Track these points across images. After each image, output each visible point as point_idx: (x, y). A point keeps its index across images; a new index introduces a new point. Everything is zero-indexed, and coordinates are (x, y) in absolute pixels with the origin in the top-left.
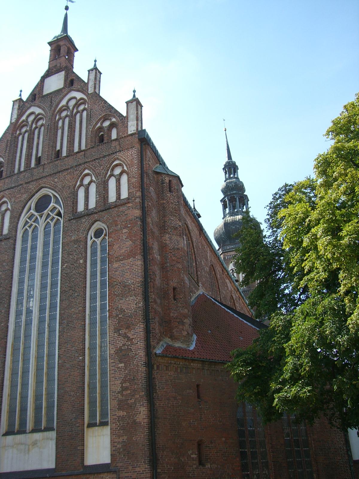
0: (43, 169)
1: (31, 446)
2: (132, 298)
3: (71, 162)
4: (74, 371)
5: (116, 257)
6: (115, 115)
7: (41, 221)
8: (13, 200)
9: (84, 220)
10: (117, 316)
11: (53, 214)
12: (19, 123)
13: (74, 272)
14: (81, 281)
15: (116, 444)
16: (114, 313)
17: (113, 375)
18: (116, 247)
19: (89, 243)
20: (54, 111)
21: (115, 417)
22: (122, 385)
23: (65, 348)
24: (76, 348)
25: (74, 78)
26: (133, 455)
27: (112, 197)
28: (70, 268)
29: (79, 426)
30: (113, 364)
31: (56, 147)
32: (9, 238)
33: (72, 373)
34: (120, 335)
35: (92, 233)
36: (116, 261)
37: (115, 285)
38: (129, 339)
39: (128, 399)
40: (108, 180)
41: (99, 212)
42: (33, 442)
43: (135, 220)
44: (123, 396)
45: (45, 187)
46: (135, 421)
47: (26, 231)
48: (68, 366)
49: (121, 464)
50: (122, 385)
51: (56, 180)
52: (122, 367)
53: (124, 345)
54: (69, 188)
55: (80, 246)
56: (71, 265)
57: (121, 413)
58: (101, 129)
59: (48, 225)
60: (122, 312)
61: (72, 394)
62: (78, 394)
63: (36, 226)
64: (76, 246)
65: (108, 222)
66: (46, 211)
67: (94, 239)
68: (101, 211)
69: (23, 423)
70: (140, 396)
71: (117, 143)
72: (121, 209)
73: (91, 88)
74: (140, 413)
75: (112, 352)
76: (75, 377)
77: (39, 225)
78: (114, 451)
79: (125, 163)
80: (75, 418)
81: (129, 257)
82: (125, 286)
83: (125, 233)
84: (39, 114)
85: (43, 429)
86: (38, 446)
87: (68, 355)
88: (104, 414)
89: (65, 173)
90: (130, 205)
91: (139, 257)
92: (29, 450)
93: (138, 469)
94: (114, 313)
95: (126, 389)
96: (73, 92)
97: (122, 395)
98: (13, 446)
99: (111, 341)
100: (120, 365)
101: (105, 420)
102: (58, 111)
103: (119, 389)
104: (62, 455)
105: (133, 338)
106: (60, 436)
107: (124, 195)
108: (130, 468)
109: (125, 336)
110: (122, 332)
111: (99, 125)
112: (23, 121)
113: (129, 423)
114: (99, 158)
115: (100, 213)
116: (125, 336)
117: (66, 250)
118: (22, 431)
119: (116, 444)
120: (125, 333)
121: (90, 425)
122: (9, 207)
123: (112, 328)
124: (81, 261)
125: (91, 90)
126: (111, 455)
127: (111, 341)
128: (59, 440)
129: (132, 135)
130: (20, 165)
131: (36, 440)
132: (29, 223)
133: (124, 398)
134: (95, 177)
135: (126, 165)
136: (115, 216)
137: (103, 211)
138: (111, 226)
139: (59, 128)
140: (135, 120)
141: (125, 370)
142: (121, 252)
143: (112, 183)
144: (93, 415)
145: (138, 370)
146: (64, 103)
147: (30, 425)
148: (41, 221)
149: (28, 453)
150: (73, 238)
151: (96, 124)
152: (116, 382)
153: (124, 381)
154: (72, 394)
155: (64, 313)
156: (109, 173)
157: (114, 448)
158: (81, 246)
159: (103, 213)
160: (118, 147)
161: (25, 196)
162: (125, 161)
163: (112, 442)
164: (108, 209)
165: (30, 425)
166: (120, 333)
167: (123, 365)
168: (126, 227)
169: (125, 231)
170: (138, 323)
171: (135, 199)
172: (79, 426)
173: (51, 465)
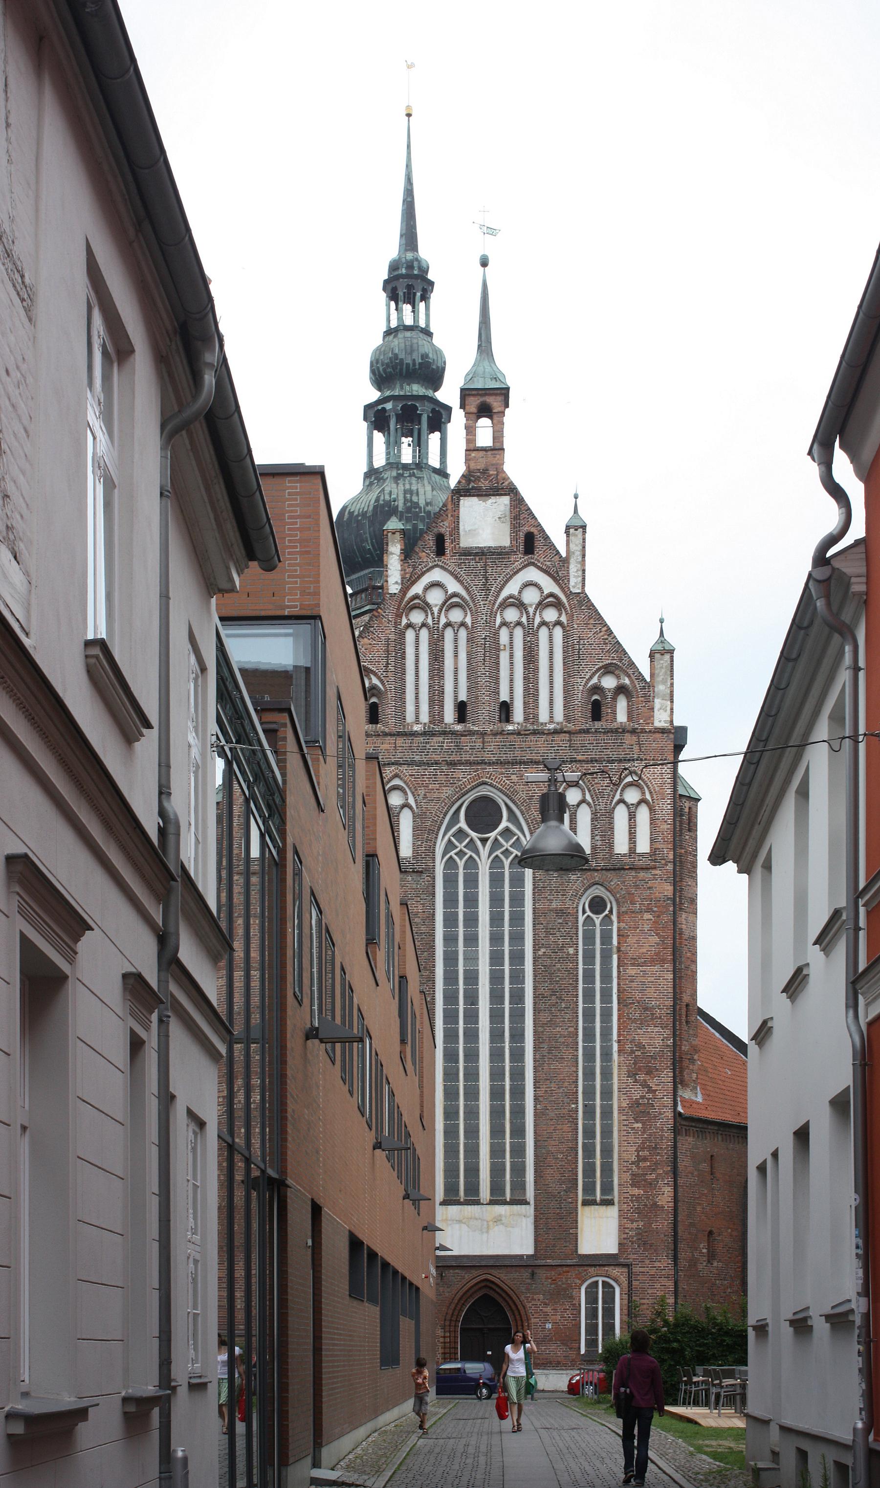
0: (483, 743)
1: (491, 1223)
2: (657, 1029)
4: (562, 1124)
5: (632, 958)
6: (630, 672)
7: (484, 851)
8: (422, 792)
9: (573, 877)
10: (633, 1052)
11: (507, 842)
12: (406, 599)
14: (571, 984)
15: (627, 1231)
16: (628, 1047)
18: (631, 940)
19: (581, 919)
20: (494, 604)
21: (626, 1195)
22: (638, 1153)
23: (547, 1088)
24: (566, 1091)
25: (533, 530)
26: (651, 1246)
27: (621, 846)
29: (572, 1203)
30: (625, 1123)
31: (497, 693)
32: (421, 872)
33: (559, 1127)
34: (636, 1081)
35: (585, 900)
36: (633, 965)
37: (630, 1003)
38: (651, 1090)
39: (647, 1174)
40: (614, 808)
41: (602, 869)
42: (494, 1218)
43: (664, 901)
44: (638, 1169)
45: (491, 785)
46: (655, 1204)
47: (451, 864)
48: (552, 1114)
49: (635, 1256)
50: (638, 1153)
51: (513, 777)
52: (638, 1128)
53: (642, 1097)
55: (567, 923)
56: (553, 952)
57: (636, 1191)
58: (597, 689)
59: (496, 863)
60: (640, 1047)
61: (560, 1156)
62: (569, 1158)
63: (471, 857)
64: (560, 921)
65: (618, 892)
66: (492, 835)
67: (589, 913)
68: (606, 870)
69: (473, 1188)
70: (664, 1171)
71: (635, 738)
72: (642, 874)
73: (575, 576)
74: (663, 1194)
76: (563, 1132)
77: (479, 857)
78: (624, 1239)
79: (648, 787)
80: (564, 1190)
81: (652, 962)
82: (646, 1009)
83: (647, 920)
84: (455, 595)
85: (508, 1200)
86: (503, 1224)
87: (553, 1098)
88: (607, 1188)
90: (658, 872)
91: (669, 966)
92: (488, 1228)
93: (657, 1264)
94: (628, 1047)
95: (645, 1159)
96: (532, 569)
97: (638, 1167)
98: (460, 1222)
99: (623, 1088)
100: (636, 1125)
101: (607, 1197)
102: (501, 605)
103: (633, 1158)
104: (546, 1239)
105: (657, 1090)
106: (542, 1214)
107: (643, 846)
108: (647, 1262)
109: (645, 1085)
110: (641, 1077)
111: (595, 680)
112: (416, 597)
113: (647, 1205)
115: (604, 872)
117: (542, 924)
118: (477, 1203)
119: (627, 1231)
120: (645, 1081)
121: (585, 1203)
122: (411, 801)
123: (625, 1069)
124: (570, 949)
126: (619, 1244)
127: (623, 1088)
128: (541, 1219)
129: (663, 731)
130: (417, 707)
131: (500, 1216)
132: (457, 847)
133: (640, 1172)
134: (592, 796)
135: (651, 793)
136: (630, 886)
137: (610, 870)
138: (624, 902)
139: (502, 647)
140: (668, 697)
141: (644, 1132)
142: (641, 951)
143: (621, 815)
144: (589, 1188)
145: (662, 1136)
146: (512, 588)
147: (485, 1192)
148: (484, 851)
149: (487, 1232)
150: (554, 905)
151: (591, 678)
152: (629, 1149)
153: (641, 1148)
154: (560, 1156)
155: (543, 1032)
156: (617, 797)
158: (570, 924)
159: (609, 875)
160: (636, 748)
161: (448, 791)
162: (649, 783)
163: (622, 1229)
164: (619, 869)
165: (485, 1192)
166: (636, 1079)
167: (640, 1125)
168: (649, 910)
169: (647, 916)
170: (665, 1069)
172: (572, 1203)
173: (530, 1251)
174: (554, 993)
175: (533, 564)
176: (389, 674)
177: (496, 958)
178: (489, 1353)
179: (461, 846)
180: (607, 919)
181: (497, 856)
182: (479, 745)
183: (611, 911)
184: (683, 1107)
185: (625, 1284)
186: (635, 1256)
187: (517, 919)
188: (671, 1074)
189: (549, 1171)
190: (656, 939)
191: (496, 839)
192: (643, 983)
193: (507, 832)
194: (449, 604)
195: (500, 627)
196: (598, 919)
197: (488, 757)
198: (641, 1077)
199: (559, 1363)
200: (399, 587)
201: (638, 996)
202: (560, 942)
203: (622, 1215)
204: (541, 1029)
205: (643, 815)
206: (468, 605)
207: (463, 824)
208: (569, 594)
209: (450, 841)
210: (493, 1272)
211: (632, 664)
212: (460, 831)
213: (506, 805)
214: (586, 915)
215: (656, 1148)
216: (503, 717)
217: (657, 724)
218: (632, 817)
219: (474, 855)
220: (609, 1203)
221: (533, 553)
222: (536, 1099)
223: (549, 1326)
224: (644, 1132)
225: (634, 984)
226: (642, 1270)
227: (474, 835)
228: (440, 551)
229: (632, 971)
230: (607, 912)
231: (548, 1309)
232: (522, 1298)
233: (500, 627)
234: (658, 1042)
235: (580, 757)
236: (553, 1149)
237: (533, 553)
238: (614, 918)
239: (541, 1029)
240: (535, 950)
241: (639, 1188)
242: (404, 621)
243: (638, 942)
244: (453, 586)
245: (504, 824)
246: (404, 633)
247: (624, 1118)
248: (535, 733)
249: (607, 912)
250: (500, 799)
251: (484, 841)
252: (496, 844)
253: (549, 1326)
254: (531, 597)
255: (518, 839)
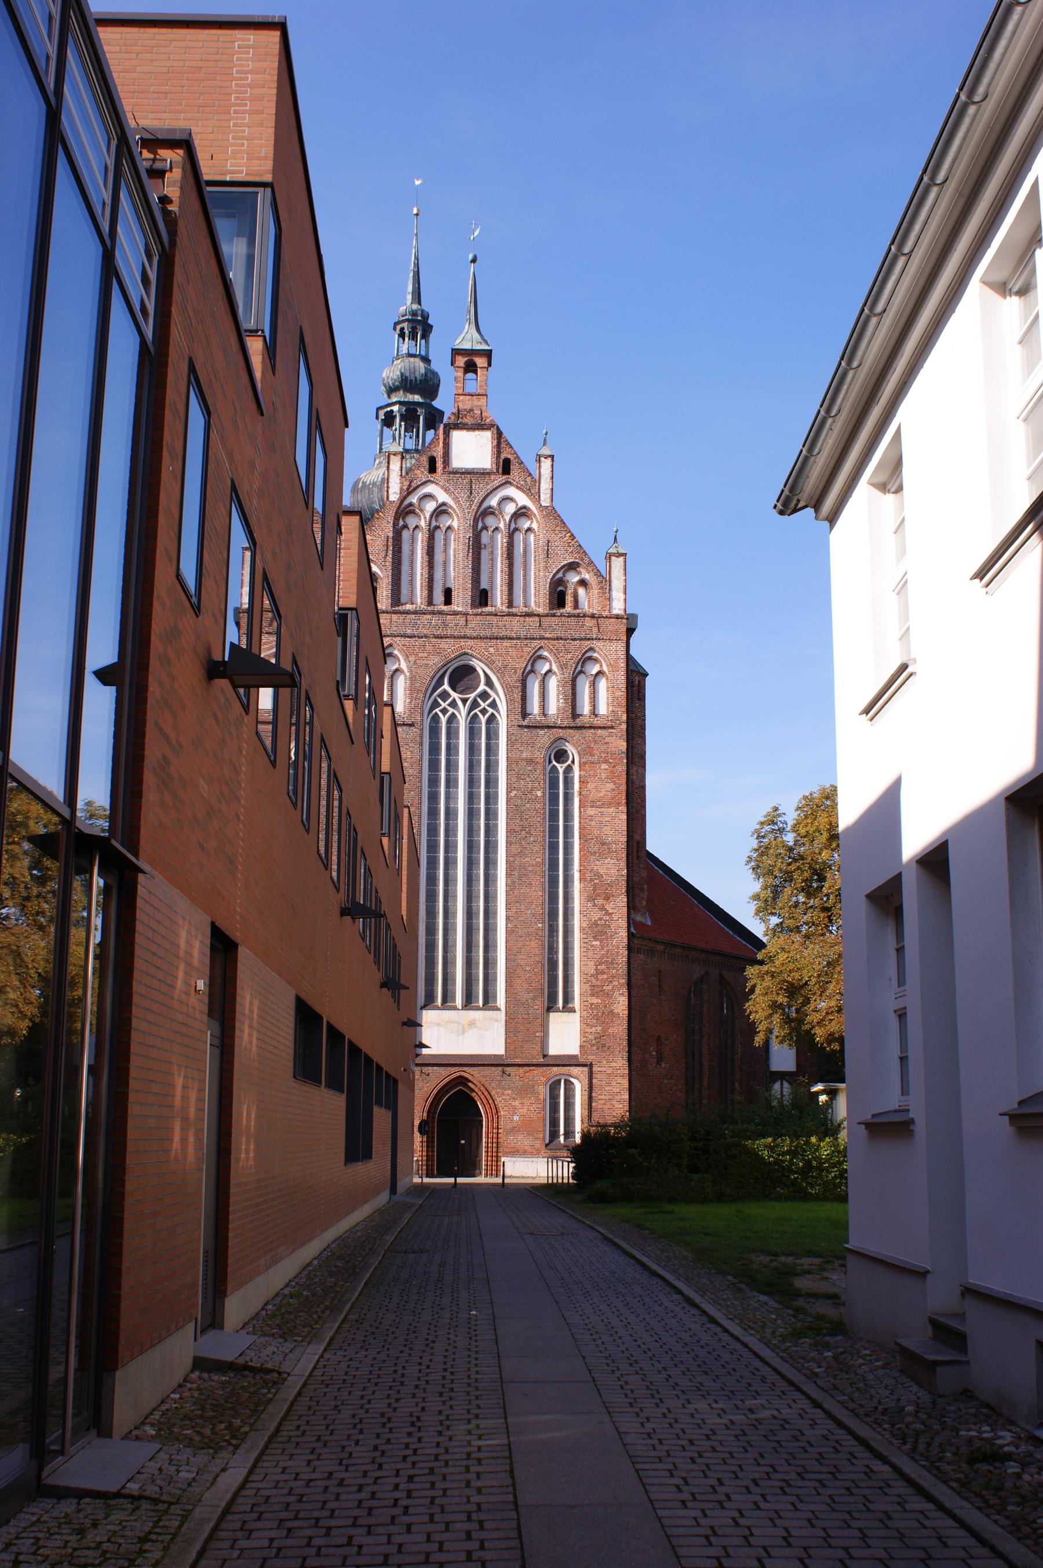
2: (612, 861)
3: (515, 626)
8: (412, 659)
10: (591, 880)
13: (528, 806)
15: (587, 1035)
16: (588, 876)
17: (585, 954)
18: (590, 786)
28: (521, 798)
30: (585, 941)
33: (527, 943)
36: (592, 807)
38: (607, 913)
51: (491, 650)
53: (600, 919)
54: (516, 672)
57: (595, 1000)
59: (473, 720)
64: (529, 768)
66: (472, 696)
71: (594, 621)
72: (600, 732)
75: (584, 925)
81: (610, 805)
82: (604, 844)
84: (444, 504)
88: (568, 998)
89: (507, 643)
93: (613, 1064)
94: (588, 876)
98: (438, 1025)
100: (594, 943)
103: (592, 971)
108: (604, 1062)
109: (603, 908)
111: (560, 575)
114: (566, 640)
116: (603, 908)
118: (455, 1008)
125: (545, 499)
129: (617, 617)
131: (474, 1020)
133: (599, 983)
139: (483, 546)
145: (618, 953)
146: (494, 502)
147: (459, 1001)
150: (524, 755)
157: (585, 1039)
160: (595, 630)
163: (583, 1033)
167: (598, 943)
168: (606, 761)
169: (604, 766)
171: (620, 724)
174: (523, 828)
175: (510, 483)
176: (387, 564)
177: (471, 798)
178: (463, 1142)
179: (444, 705)
180: (569, 770)
181: (476, 713)
182: (462, 621)
183: (573, 762)
184: (635, 928)
185: (586, 1081)
186: (593, 1057)
187: (491, 766)
188: (626, 900)
189: (519, 981)
190: (611, 786)
191: (475, 700)
192: (601, 822)
193: (484, 695)
194: (441, 511)
195: (481, 530)
196: (561, 768)
197: (468, 632)
198: (600, 901)
199: (525, 1151)
200: (398, 496)
201: (596, 832)
202: (529, 786)
203: (584, 1021)
204: (511, 859)
205: (602, 685)
206: (455, 512)
207: (446, 686)
208: (540, 507)
209: (435, 700)
210: (465, 1069)
211: (591, 563)
212: (445, 692)
213: (484, 672)
214: (551, 765)
215: (612, 963)
216: (483, 601)
217: (615, 612)
218: (594, 685)
219: (456, 712)
220: (573, 1010)
221: (509, 474)
222: (507, 918)
223: (516, 1118)
224: (602, 949)
225: (593, 823)
226: (599, 1069)
227: (454, 695)
228: (432, 469)
229: (591, 811)
230: (569, 762)
231: (516, 1103)
232: (493, 1093)
233: (481, 530)
234: (614, 872)
235: (547, 635)
236: (522, 963)
237: (509, 474)
238: (576, 768)
239: (511, 859)
240: (508, 792)
241: (597, 997)
242: (401, 523)
243: (596, 788)
244: (442, 497)
245: (482, 687)
246: (401, 533)
247: (585, 936)
248: (509, 615)
249: (569, 762)
250: (479, 666)
251: (464, 701)
252: (475, 704)
253: (516, 1118)
254: (510, 509)
255: (494, 700)
